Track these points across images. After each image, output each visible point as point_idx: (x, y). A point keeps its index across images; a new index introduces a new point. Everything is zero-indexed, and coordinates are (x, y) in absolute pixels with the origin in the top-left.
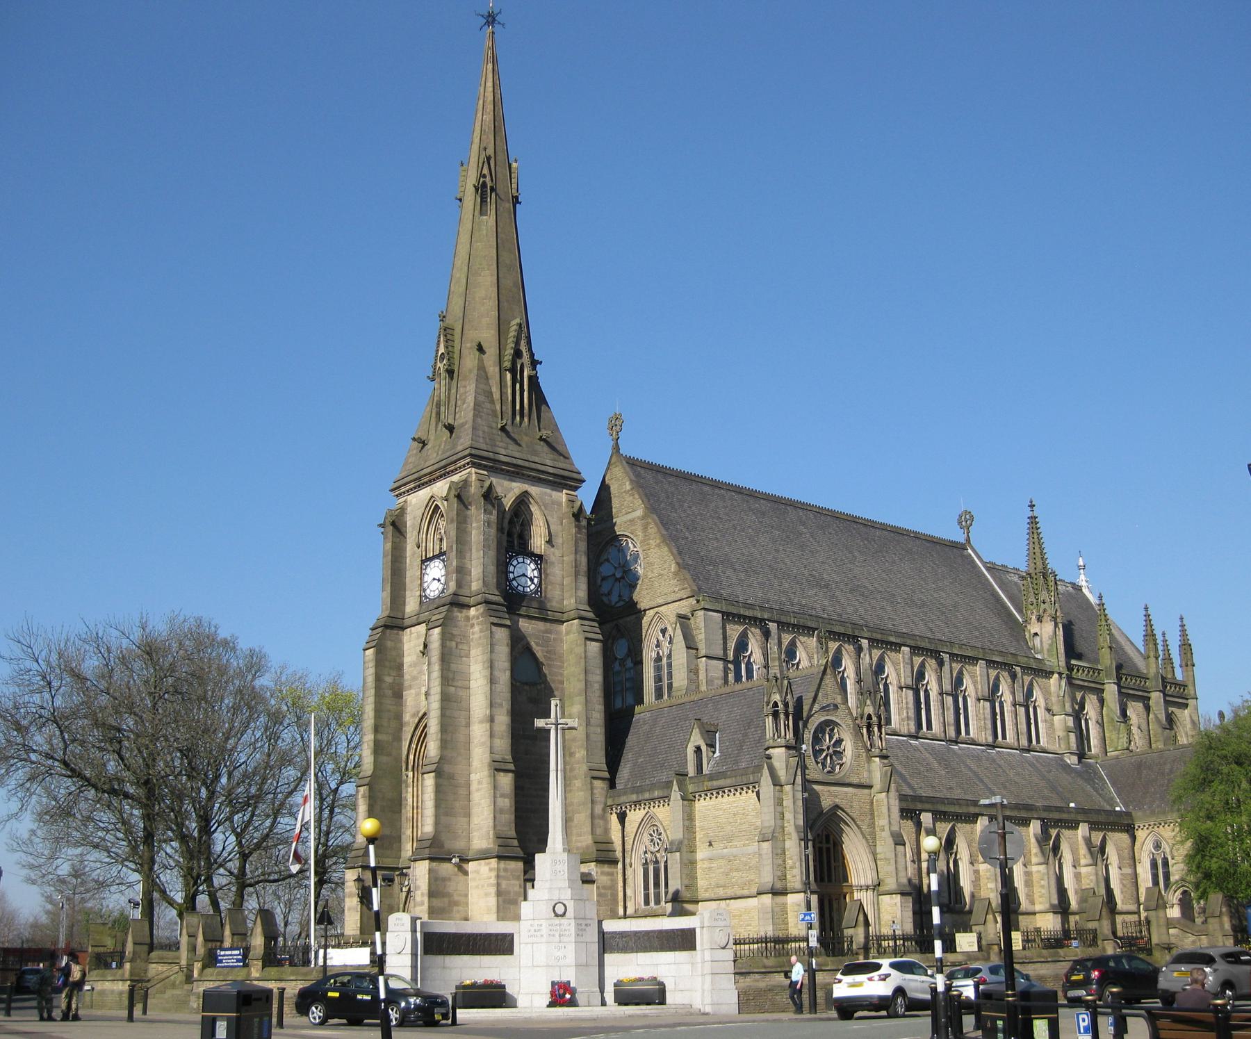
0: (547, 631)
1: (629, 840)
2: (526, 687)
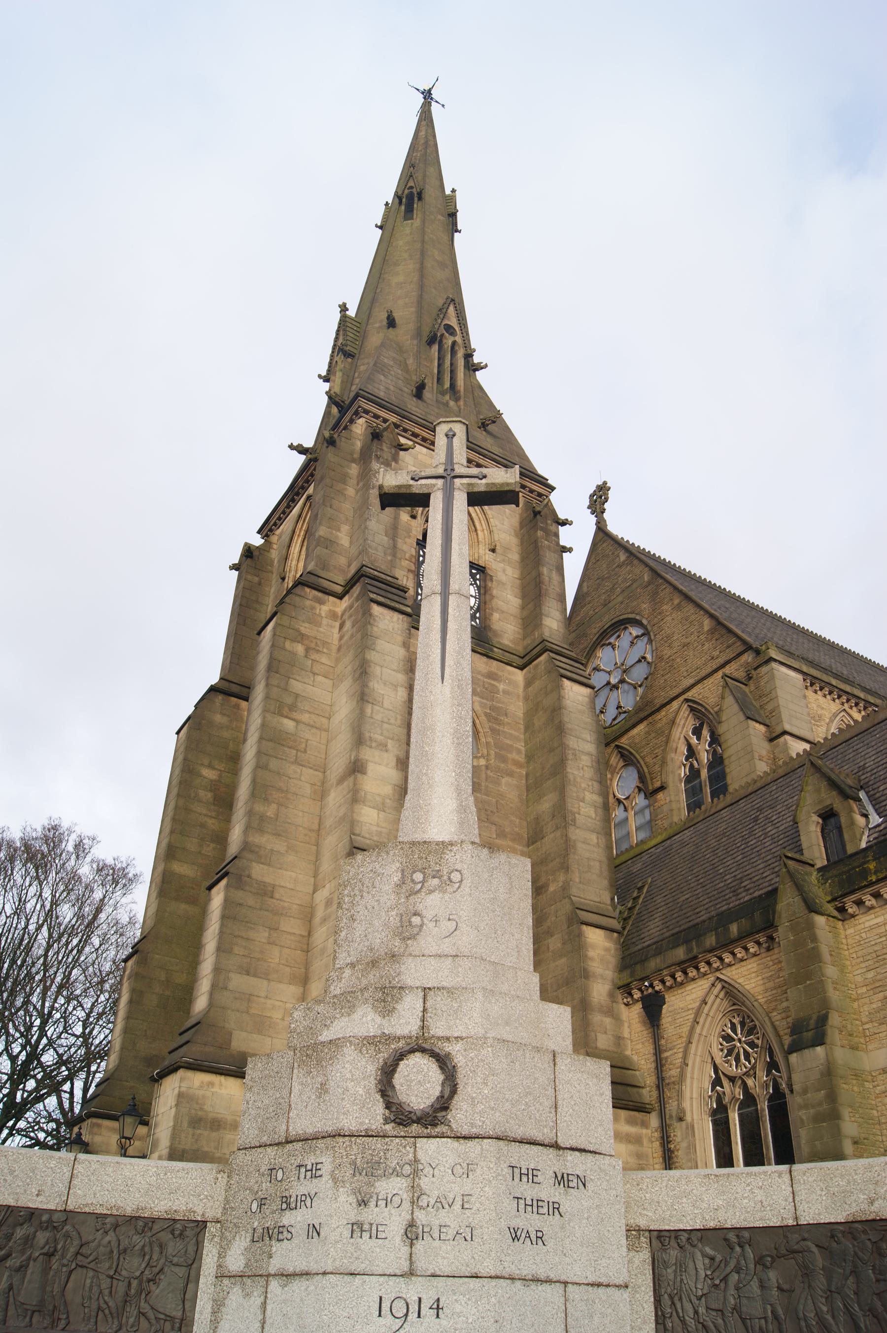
0: (491, 676)
1: (673, 1057)
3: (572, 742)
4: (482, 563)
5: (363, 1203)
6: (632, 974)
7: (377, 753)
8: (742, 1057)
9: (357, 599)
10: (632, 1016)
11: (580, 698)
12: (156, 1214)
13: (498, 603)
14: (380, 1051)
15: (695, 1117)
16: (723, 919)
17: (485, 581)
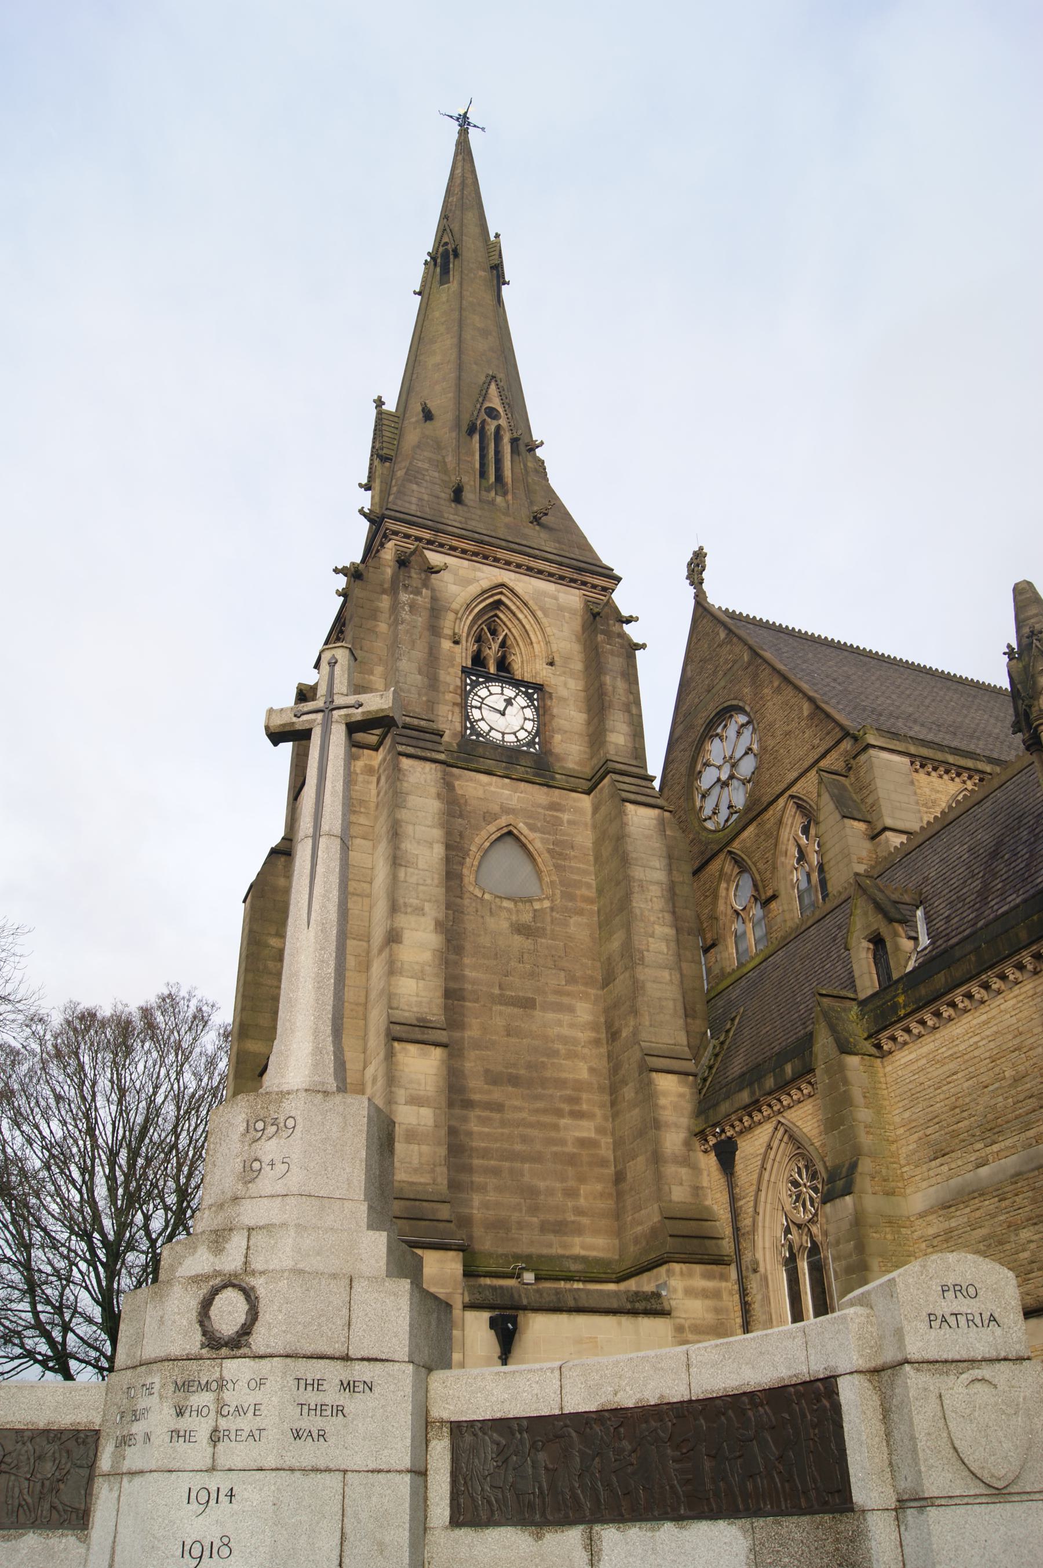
0: (554, 807)
1: (746, 1204)
2: (506, 904)
3: (638, 873)
4: (539, 681)
5: (180, 1413)
6: (706, 1121)
7: (412, 919)
8: (808, 1203)
9: (389, 752)
10: (709, 1163)
11: (647, 822)
12: (63, 1427)
13: (560, 722)
14: (200, 1288)
15: (769, 1267)
16: (783, 1057)
17: (543, 699)
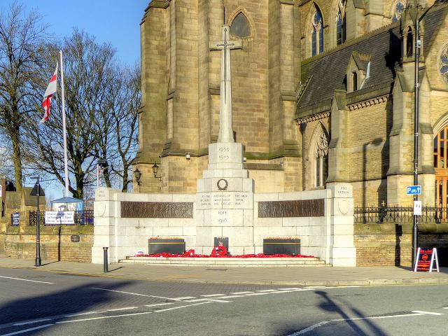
1: (307, 142)
10: (297, 128)
